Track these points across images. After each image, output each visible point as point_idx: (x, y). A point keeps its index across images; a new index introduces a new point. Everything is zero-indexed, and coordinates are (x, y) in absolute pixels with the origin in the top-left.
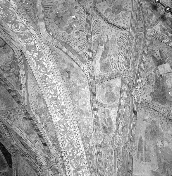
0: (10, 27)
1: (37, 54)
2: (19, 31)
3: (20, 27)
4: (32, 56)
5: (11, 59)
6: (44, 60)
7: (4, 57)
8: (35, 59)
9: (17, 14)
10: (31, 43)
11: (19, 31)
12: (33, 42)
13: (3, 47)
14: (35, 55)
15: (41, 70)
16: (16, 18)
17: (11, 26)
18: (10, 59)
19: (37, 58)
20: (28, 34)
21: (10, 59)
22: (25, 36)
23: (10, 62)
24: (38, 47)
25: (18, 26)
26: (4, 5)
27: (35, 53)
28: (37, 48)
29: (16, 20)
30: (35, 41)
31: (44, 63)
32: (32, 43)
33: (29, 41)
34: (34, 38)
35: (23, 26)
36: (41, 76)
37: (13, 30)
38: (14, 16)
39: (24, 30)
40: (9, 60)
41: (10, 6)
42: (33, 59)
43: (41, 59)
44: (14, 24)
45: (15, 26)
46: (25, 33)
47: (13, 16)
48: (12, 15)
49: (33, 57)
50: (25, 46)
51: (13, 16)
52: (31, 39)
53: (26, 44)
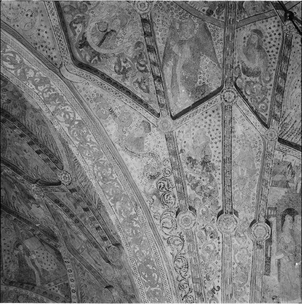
0: (77, 115)
1: (28, 76)
2: (63, 108)
3: (63, 114)
4: (35, 72)
5: (88, 15)
6: (13, 72)
7: (105, 14)
8: (29, 68)
9: (69, 135)
10: (43, 88)
11: (63, 108)
12: (41, 90)
13: (108, 33)
14: (31, 74)
15: (12, 55)
16: (69, 128)
17: (75, 116)
18: (91, 14)
19: (26, 70)
20: (49, 103)
21: (91, 14)
22: (54, 99)
23: (92, 9)
24: (29, 86)
25: (64, 116)
26: (85, 149)
27: (32, 76)
28: (31, 84)
29: (68, 125)
30: (37, 92)
31: (12, 67)
32: (41, 88)
33: (46, 90)
34: (41, 97)
35: (58, 117)
36: (8, 47)
37: (72, 110)
38: (72, 131)
39: (56, 110)
40: (93, 12)
41: (77, 146)
42: (33, 67)
43: (19, 71)
44: (72, 119)
45: (69, 116)
46: (54, 105)
47: (74, 132)
48: (75, 133)
49: (33, 69)
50: (51, 83)
51: (74, 132)
52: (44, 94)
53: (51, 85)
